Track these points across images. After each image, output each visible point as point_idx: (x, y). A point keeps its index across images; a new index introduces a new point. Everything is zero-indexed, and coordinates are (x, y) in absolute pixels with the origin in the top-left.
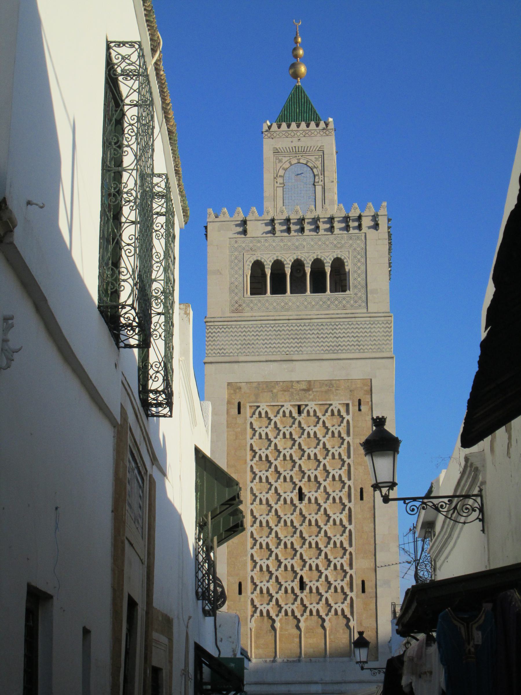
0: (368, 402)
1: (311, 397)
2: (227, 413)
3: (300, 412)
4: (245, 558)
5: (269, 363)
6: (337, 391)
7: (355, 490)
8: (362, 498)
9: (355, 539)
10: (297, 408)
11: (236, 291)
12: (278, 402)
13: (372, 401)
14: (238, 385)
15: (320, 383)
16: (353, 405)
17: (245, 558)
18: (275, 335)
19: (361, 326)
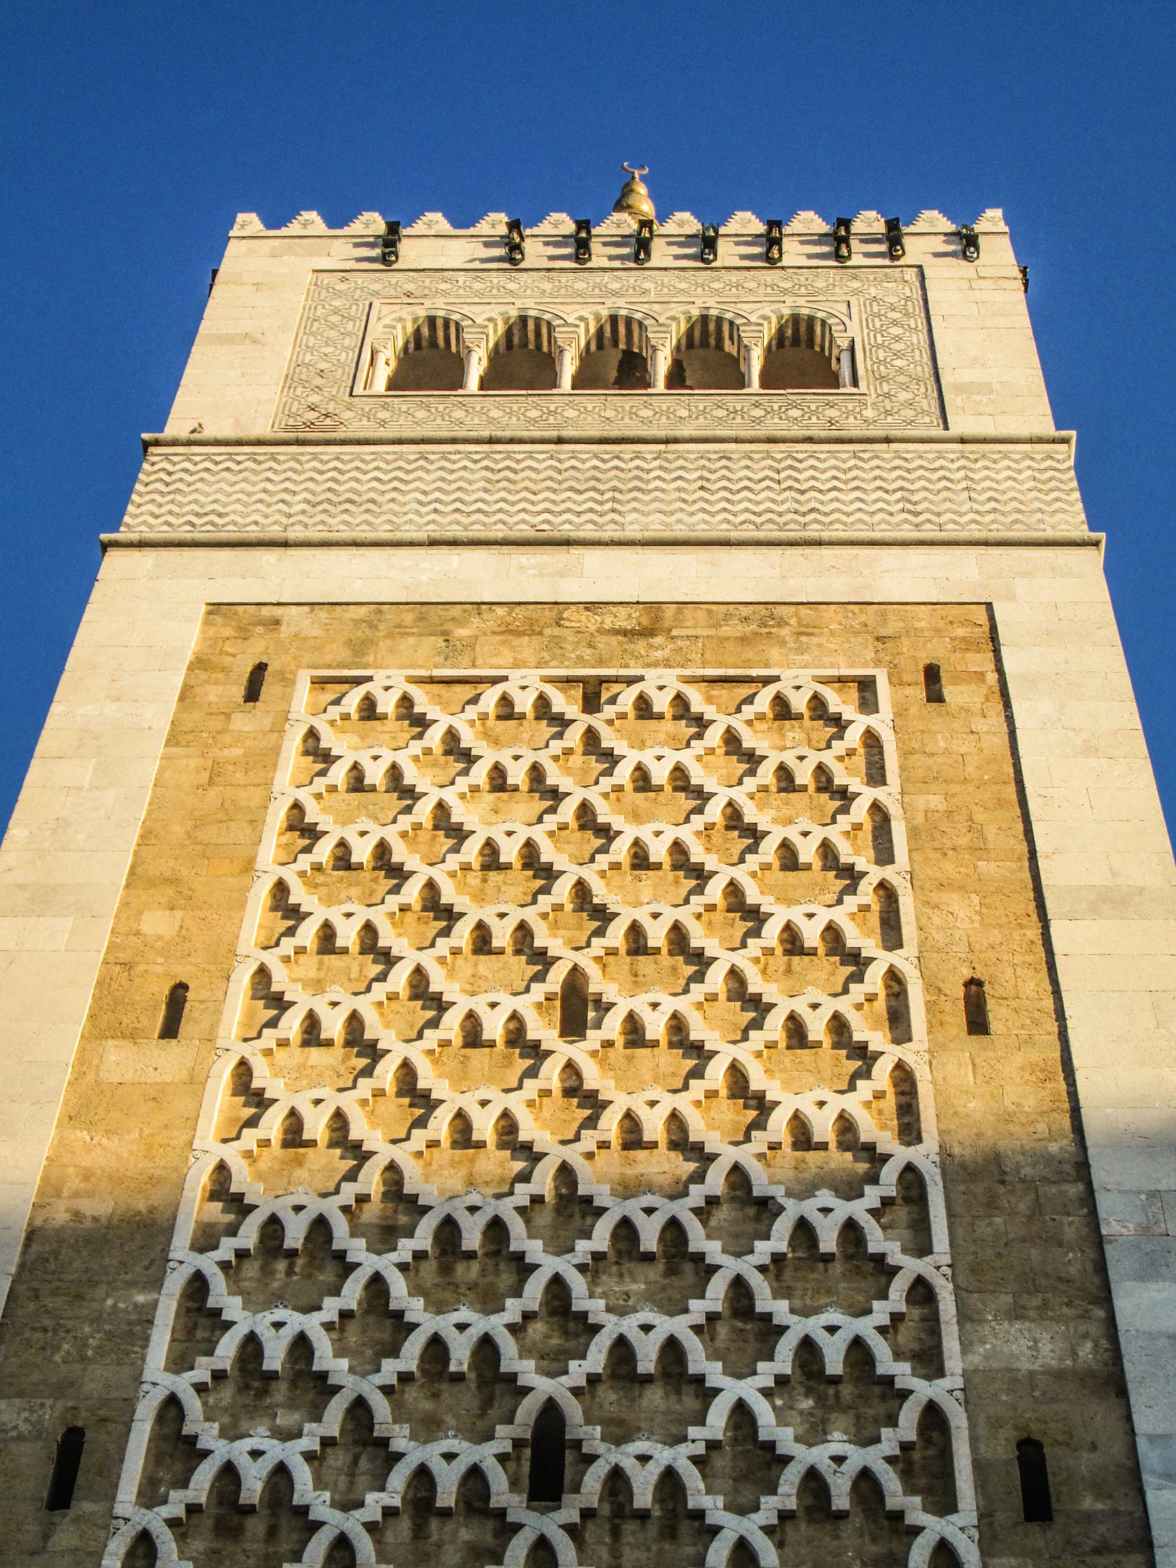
0: (981, 676)
1: (659, 654)
2: (182, 698)
3: (591, 704)
4: (141, 1298)
5: (445, 550)
6: (804, 639)
7: (932, 987)
8: (978, 1023)
9: (951, 1215)
10: (578, 692)
11: (319, 381)
12: (474, 666)
13: (1000, 670)
14: (266, 612)
15: (709, 612)
16: (896, 681)
17: (141, 1298)
18: (488, 481)
19: (919, 462)
